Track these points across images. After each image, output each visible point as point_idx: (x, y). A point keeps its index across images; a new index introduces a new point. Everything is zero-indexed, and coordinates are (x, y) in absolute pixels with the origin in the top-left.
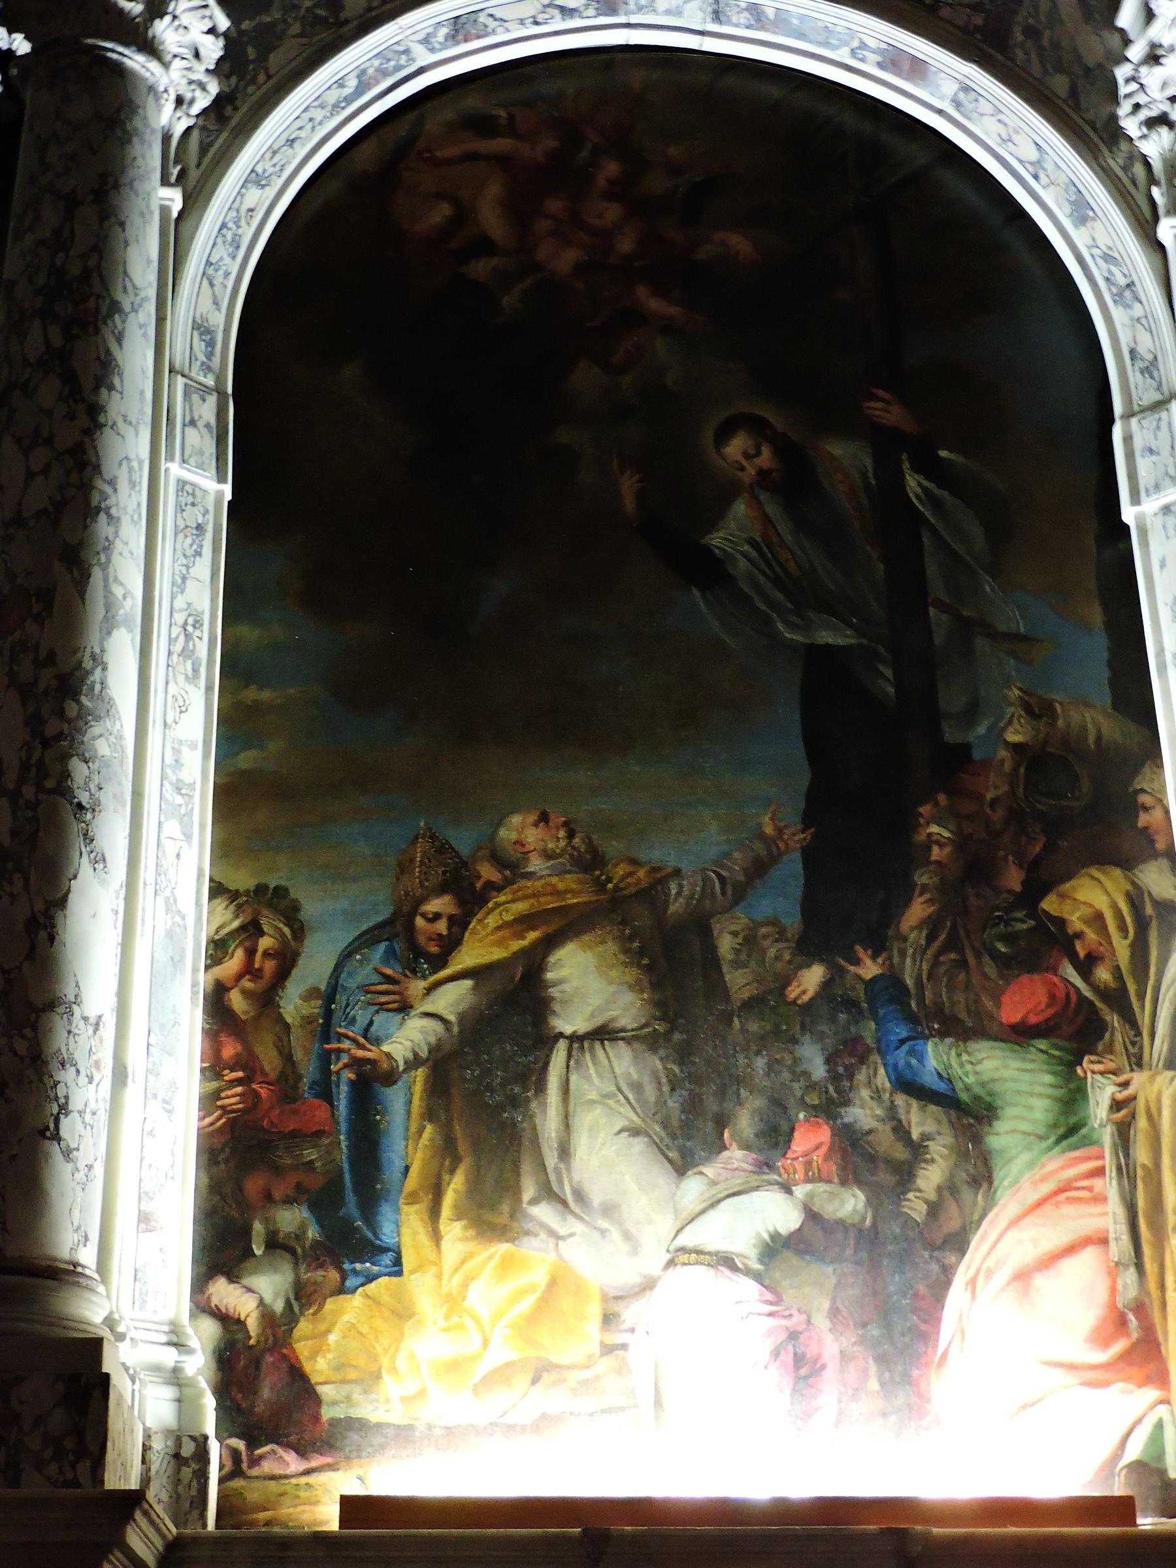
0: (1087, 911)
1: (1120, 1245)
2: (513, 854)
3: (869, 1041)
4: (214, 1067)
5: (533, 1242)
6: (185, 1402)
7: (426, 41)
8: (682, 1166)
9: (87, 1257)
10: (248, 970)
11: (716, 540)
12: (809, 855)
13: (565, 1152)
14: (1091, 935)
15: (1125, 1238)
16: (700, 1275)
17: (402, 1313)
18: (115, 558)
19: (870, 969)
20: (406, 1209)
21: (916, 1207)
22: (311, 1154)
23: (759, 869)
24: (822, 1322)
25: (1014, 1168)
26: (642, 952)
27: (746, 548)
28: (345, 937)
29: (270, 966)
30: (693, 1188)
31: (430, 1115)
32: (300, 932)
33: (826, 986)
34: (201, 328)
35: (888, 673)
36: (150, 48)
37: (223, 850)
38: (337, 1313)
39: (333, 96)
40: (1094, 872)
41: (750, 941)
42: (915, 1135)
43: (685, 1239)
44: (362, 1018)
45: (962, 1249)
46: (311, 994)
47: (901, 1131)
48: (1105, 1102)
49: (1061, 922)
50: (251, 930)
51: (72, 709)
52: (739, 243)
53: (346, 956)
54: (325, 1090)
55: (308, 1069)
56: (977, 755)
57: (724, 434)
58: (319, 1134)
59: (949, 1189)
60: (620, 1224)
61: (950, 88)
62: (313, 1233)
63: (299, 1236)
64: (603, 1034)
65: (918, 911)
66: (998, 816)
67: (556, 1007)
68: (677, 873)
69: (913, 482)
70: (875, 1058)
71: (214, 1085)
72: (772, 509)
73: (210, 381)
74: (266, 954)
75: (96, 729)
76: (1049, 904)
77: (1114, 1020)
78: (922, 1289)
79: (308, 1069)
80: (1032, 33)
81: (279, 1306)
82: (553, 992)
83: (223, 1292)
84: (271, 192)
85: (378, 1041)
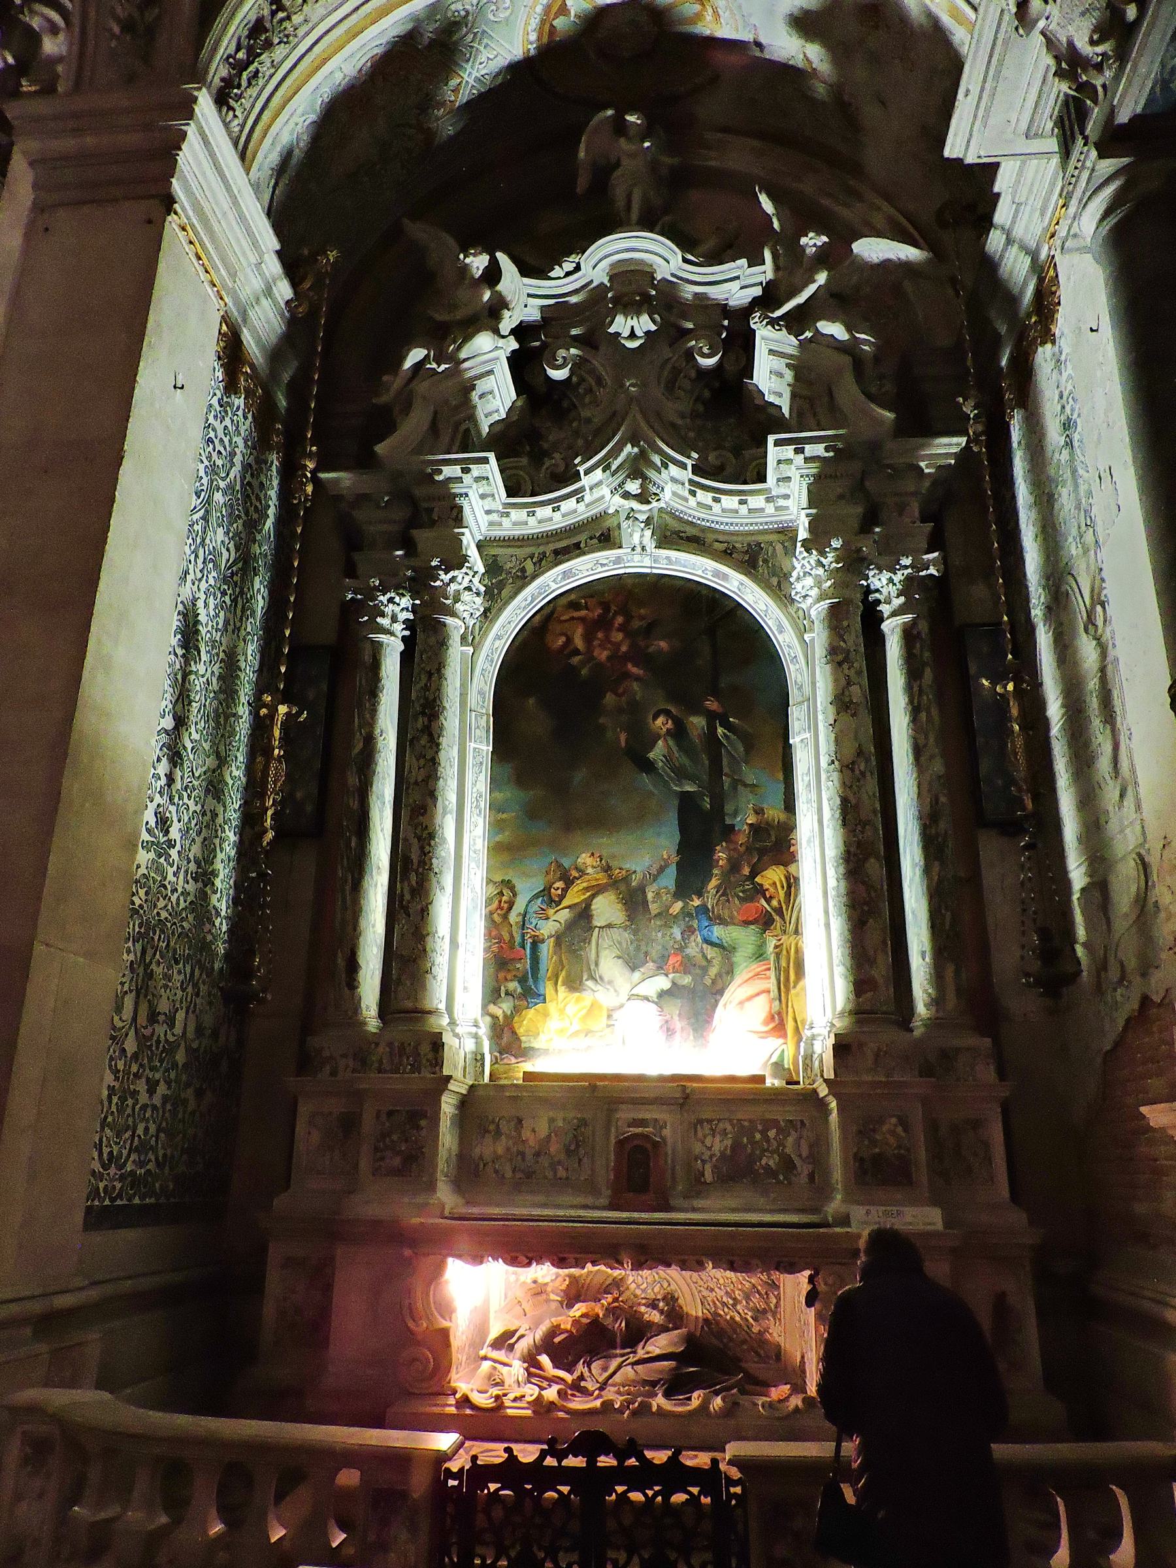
0: (771, 882)
1: (774, 993)
2: (583, 867)
3: (696, 926)
4: (489, 936)
5: (586, 993)
6: (478, 1043)
7: (554, 581)
8: (633, 969)
10: (500, 907)
11: (651, 755)
12: (680, 866)
13: (597, 964)
14: (772, 890)
15: (776, 991)
17: (546, 1015)
18: (446, 792)
19: (697, 902)
20: (548, 983)
23: (661, 870)
24: (676, 1018)
25: (741, 967)
26: (623, 899)
27: (662, 758)
29: (506, 906)
30: (637, 975)
32: (515, 895)
34: (481, 693)
35: (708, 800)
36: (453, 614)
38: (526, 1015)
40: (774, 867)
42: (709, 958)
43: (634, 992)
45: (722, 995)
47: (704, 956)
48: (773, 946)
49: (761, 885)
50: (501, 894)
51: (433, 843)
52: (663, 644)
53: (530, 902)
55: (518, 939)
57: (655, 718)
58: (521, 959)
59: (719, 975)
60: (614, 987)
61: (736, 584)
62: (519, 990)
64: (609, 926)
65: (714, 882)
66: (742, 849)
67: (595, 917)
68: (635, 872)
69: (720, 730)
70: (697, 932)
71: (489, 944)
72: (671, 742)
73: (484, 711)
74: (505, 902)
75: (440, 849)
77: (777, 918)
78: (708, 1007)
79: (518, 939)
80: (765, 561)
81: (509, 1013)
82: (594, 912)
83: (493, 1009)
84: (503, 641)
85: (539, 929)
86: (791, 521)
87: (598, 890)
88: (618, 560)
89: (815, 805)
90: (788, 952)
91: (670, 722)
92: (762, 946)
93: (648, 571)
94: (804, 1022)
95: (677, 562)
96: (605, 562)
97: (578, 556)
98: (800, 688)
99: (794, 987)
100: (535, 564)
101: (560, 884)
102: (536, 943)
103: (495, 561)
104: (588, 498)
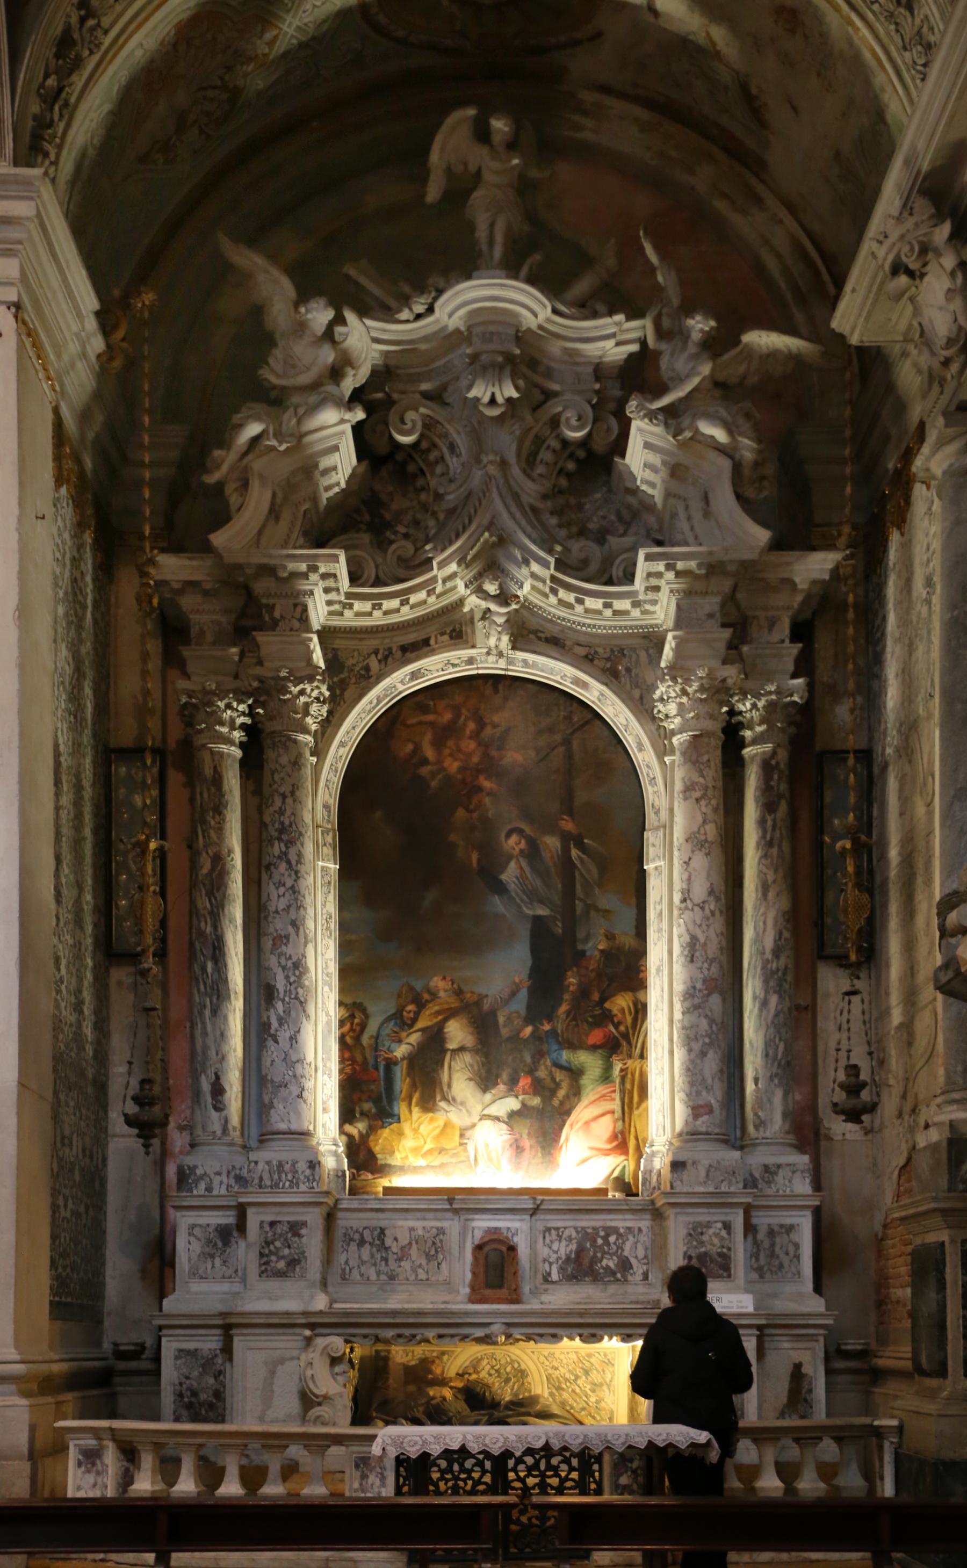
4: (342, 1060)
7: (402, 682)
8: (485, 1090)
9: (311, 1128)
10: (352, 1030)
11: (503, 877)
13: (449, 1086)
14: (620, 1015)
16: (487, 1123)
19: (547, 1027)
21: (556, 1102)
22: (373, 1087)
23: (513, 994)
24: (525, 1136)
28: (381, 1019)
29: (358, 1028)
30: (488, 1097)
31: (408, 1074)
32: (367, 1016)
33: (533, 1033)
34: (326, 807)
35: (560, 924)
37: (342, 991)
39: (368, 708)
41: (509, 1019)
43: (485, 1112)
44: (387, 1044)
46: (372, 1037)
47: (553, 1079)
49: (610, 1011)
50: (352, 1016)
53: (382, 1024)
54: (376, 1067)
56: (588, 954)
59: (567, 1097)
62: (374, 1110)
63: (370, 1111)
64: (462, 1049)
65: (564, 1008)
66: (593, 975)
69: (574, 853)
76: (607, 1005)
77: (624, 1043)
79: (371, 1061)
83: (348, 1128)
84: (347, 748)
86: (657, 626)
87: (450, 1014)
88: (471, 661)
89: (666, 935)
90: (633, 1075)
91: (523, 841)
92: (608, 1068)
93: (502, 672)
94: (645, 1140)
95: (534, 666)
96: (456, 662)
97: (425, 656)
98: (657, 813)
99: (638, 1108)
100: (380, 661)
101: (411, 1007)
102: (390, 1064)
103: (336, 657)
104: (439, 589)
